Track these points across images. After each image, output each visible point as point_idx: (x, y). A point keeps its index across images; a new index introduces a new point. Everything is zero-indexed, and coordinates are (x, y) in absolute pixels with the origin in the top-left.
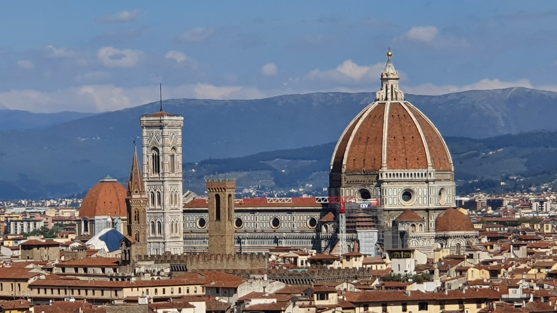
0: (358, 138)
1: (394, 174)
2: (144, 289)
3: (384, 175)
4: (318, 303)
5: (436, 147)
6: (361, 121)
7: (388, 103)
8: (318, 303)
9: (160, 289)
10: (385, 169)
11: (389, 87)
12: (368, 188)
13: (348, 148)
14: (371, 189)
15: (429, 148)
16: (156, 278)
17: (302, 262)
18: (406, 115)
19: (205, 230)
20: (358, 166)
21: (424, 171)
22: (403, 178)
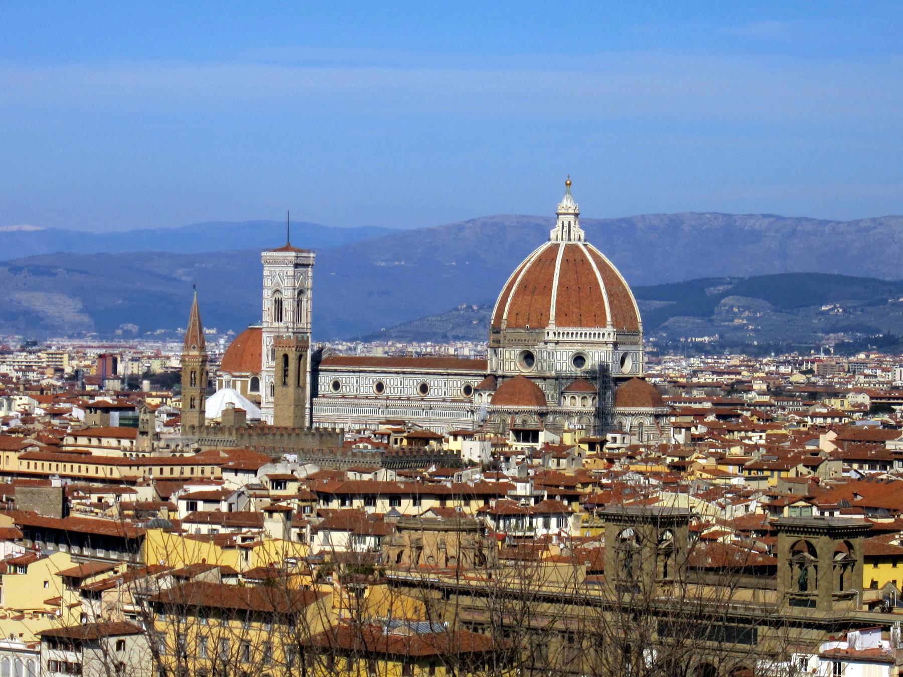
0: (523, 286)
1: (559, 333)
2: (147, 468)
3: (551, 334)
4: (273, 492)
5: (619, 301)
6: (528, 265)
7: (563, 245)
8: (273, 492)
9: (167, 469)
10: (552, 327)
11: (566, 224)
12: (531, 350)
13: (509, 299)
14: (534, 351)
15: (611, 303)
16: (178, 455)
17: (396, 440)
18: (584, 261)
19: (339, 395)
20: (521, 322)
21: (602, 331)
22: (588, 339)
